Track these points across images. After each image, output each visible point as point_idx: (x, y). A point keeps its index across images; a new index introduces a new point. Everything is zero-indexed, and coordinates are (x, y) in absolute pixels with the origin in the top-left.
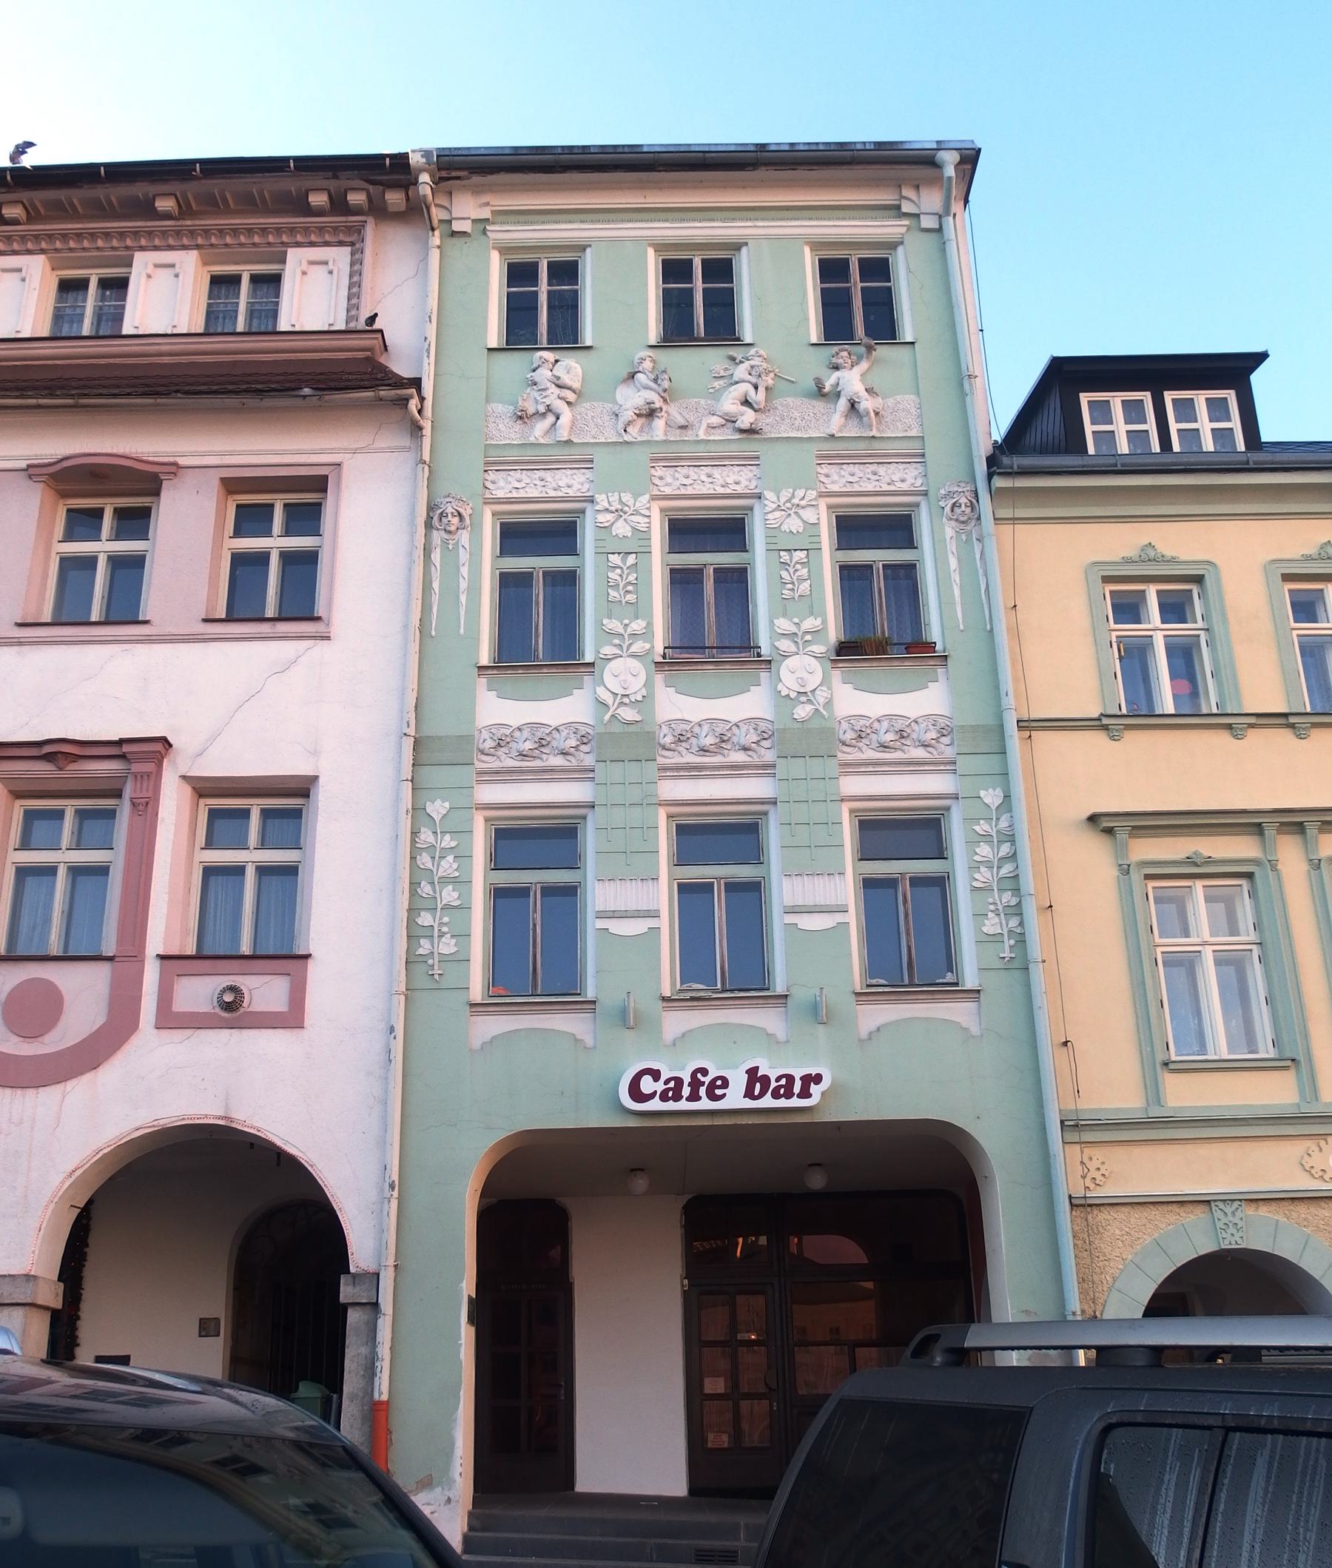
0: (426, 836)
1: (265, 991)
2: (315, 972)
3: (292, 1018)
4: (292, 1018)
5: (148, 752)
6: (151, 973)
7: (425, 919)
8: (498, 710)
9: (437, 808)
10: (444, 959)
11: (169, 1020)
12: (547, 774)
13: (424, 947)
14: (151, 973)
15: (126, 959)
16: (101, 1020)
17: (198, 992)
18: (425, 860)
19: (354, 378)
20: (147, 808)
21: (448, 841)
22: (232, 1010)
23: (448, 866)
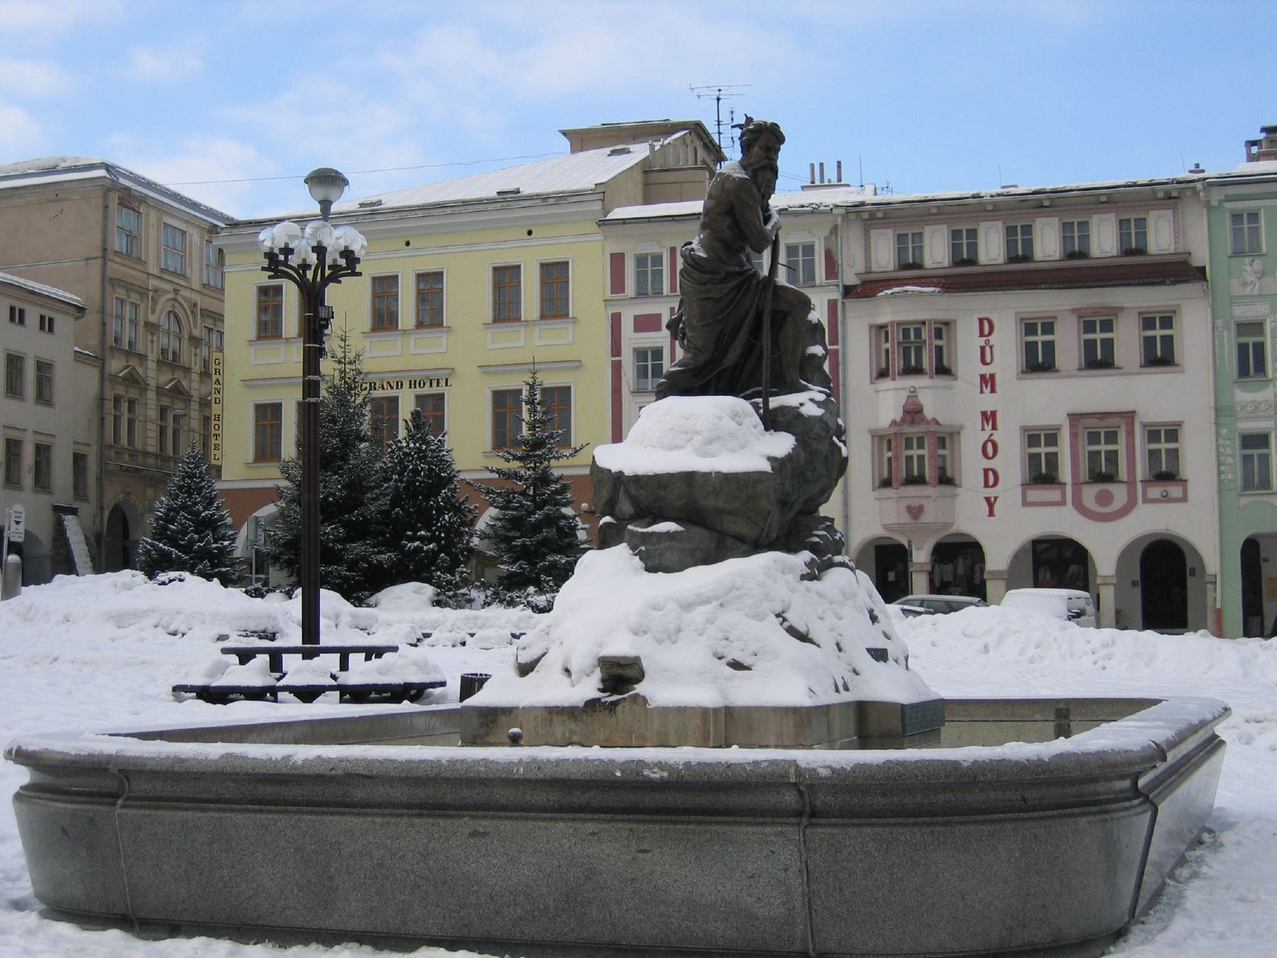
0: (1221, 441)
1: (1175, 491)
2: (1190, 484)
3: (1184, 499)
4: (1184, 499)
5: (1129, 416)
6: (1139, 487)
7: (1223, 468)
8: (1243, 396)
9: (1224, 431)
10: (1229, 481)
11: (1146, 500)
12: (1259, 418)
13: (1223, 477)
14: (1139, 487)
15: (1131, 483)
16: (1126, 500)
17: (1155, 491)
18: (1222, 449)
19: (1179, 271)
20: (1130, 433)
21: (1228, 443)
22: (1166, 499)
23: (1229, 451)
